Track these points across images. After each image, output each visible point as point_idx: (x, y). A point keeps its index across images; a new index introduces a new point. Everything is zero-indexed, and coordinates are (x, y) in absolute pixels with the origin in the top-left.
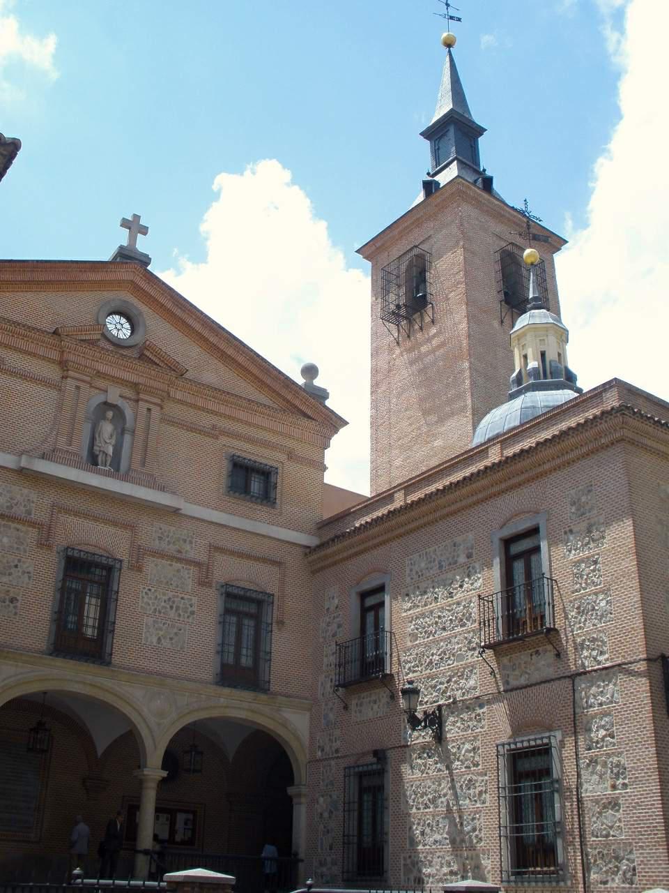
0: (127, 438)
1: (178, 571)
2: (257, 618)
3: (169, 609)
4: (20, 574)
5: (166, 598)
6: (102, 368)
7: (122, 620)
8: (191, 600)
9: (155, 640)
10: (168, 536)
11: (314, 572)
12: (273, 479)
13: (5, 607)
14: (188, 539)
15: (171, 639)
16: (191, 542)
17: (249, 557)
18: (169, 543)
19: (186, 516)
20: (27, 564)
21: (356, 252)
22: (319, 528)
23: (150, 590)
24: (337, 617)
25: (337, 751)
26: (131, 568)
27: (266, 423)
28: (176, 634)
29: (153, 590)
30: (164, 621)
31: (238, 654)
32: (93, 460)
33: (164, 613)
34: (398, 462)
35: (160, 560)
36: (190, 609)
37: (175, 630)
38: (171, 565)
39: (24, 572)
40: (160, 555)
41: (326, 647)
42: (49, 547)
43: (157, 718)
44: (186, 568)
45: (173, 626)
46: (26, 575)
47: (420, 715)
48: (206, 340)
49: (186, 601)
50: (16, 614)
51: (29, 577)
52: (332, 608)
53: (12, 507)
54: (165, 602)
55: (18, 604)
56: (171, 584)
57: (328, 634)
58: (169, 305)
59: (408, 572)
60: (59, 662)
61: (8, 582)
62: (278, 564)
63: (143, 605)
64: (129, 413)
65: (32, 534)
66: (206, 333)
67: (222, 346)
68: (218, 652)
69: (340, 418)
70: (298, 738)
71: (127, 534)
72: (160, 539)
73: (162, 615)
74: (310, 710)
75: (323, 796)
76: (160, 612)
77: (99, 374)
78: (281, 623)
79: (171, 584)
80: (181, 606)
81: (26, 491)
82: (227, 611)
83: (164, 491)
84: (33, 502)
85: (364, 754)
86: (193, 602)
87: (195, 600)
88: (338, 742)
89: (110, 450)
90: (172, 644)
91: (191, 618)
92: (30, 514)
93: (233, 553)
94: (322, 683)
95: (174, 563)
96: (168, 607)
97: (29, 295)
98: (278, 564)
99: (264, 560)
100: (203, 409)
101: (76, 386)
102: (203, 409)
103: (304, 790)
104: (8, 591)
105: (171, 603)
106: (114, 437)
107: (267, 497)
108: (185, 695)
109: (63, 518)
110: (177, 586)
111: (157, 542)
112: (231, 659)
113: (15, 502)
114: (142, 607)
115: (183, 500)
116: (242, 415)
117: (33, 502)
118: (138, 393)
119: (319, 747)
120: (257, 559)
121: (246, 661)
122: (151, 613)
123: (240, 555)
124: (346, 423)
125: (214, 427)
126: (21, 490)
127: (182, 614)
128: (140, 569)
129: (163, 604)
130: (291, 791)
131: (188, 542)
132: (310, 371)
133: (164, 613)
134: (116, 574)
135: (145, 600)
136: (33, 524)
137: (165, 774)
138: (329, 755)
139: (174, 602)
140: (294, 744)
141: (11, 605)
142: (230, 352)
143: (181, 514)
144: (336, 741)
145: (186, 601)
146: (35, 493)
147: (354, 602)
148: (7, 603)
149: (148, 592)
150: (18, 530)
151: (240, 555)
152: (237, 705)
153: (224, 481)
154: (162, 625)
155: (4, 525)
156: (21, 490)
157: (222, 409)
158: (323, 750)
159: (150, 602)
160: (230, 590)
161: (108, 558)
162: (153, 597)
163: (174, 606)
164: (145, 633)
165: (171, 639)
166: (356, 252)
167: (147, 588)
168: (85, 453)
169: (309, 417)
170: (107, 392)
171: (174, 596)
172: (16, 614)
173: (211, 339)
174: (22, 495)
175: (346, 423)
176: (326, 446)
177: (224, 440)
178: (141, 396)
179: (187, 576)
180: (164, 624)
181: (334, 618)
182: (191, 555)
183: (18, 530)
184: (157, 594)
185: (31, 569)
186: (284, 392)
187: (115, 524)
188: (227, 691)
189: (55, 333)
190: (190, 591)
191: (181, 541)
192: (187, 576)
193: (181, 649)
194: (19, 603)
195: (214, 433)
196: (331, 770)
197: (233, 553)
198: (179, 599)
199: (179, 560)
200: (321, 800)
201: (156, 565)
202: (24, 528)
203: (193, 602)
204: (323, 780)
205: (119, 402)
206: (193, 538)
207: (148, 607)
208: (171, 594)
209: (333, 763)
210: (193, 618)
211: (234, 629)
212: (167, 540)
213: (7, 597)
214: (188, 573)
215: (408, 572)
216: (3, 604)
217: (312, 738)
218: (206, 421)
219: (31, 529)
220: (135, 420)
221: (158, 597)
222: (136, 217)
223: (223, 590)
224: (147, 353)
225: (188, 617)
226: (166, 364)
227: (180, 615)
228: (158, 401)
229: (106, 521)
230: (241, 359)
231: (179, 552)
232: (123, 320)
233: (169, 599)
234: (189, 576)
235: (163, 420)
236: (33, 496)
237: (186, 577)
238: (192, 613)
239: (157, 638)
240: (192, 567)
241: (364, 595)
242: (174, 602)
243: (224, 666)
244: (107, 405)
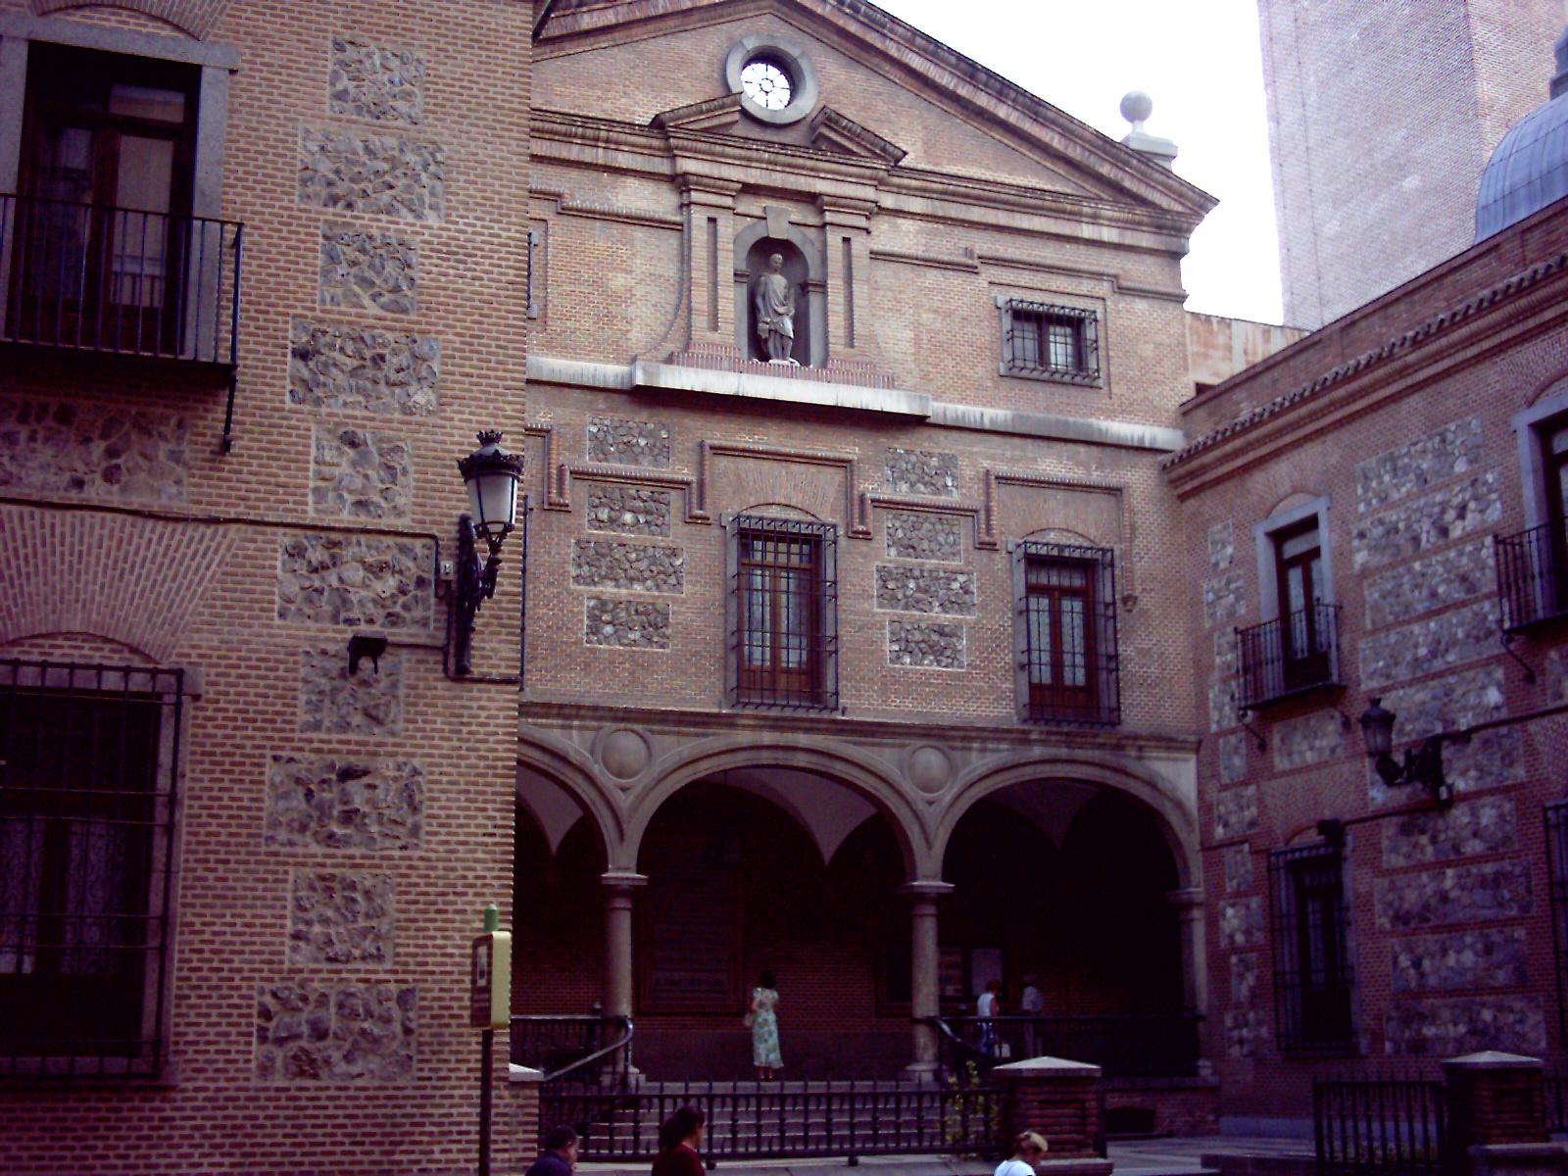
0: (814, 300)
2: (1087, 595)
11: (1183, 497)
22: (1185, 414)
26: (854, 535)
31: (1057, 665)
32: (759, 349)
34: (1331, 228)
43: (932, 795)
47: (1399, 758)
64: (810, 254)
69: (1204, 195)
70: (1179, 805)
82: (1032, 589)
85: (1300, 831)
107: (1082, 372)
108: (970, 749)
112: (1046, 676)
121: (1080, 678)
124: (1216, 202)
125: (968, 253)
132: (1134, 109)
134: (829, 552)
140: (1174, 818)
147: (1263, 554)
158: (1226, 825)
160: (1033, 550)
175: (1216, 202)
178: (829, 217)
205: (794, 236)
211: (1045, 619)
223: (1021, 552)
232: (773, 72)
241: (1279, 537)
243: (1035, 689)
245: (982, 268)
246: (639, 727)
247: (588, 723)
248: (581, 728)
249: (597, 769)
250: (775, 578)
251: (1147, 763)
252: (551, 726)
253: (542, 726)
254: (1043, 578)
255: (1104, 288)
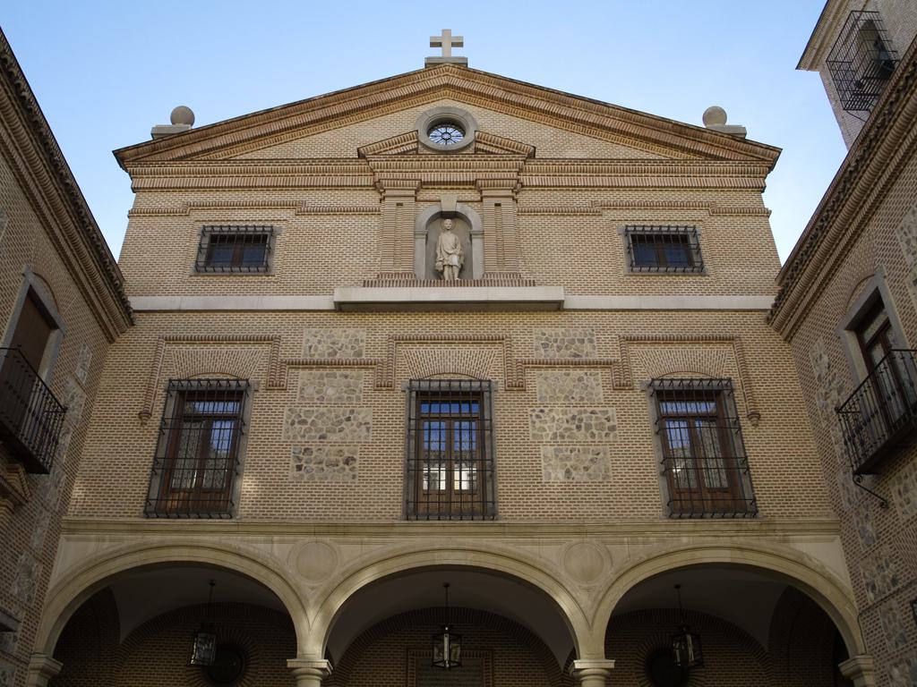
0: (477, 242)
1: (580, 379)
3: (575, 431)
4: (354, 427)
5: (570, 415)
6: (426, 177)
7: (505, 458)
8: (607, 412)
9: (561, 475)
10: (556, 341)
11: (788, 339)
12: (692, 241)
13: (338, 471)
14: (586, 339)
15: (586, 469)
16: (591, 341)
17: (681, 340)
18: (559, 348)
19: (576, 310)
20: (363, 415)
21: (797, 68)
23: (542, 411)
24: (833, 379)
25: (894, 581)
26: (510, 388)
27: (666, 181)
28: (592, 460)
29: (546, 410)
30: (570, 447)
32: (438, 276)
33: (569, 437)
35: (550, 371)
36: (608, 424)
37: (590, 456)
38: (568, 375)
39: (361, 424)
40: (552, 365)
41: (833, 430)
42: (389, 387)
44: (591, 374)
45: (586, 451)
46: (364, 427)
48: (559, 116)
49: (599, 415)
50: (354, 477)
51: (368, 429)
52: (825, 371)
53: (336, 353)
54: (567, 422)
55: (356, 465)
56: (573, 398)
57: (829, 410)
58: (500, 94)
59: (904, 247)
60: (419, 526)
61: (340, 441)
62: (730, 340)
63: (536, 432)
65: (363, 379)
66: (555, 109)
67: (580, 115)
68: (663, 474)
69: (768, 147)
70: (830, 580)
71: (497, 350)
72: (545, 346)
73: (566, 439)
74: (837, 531)
75: (896, 665)
76: (562, 437)
77: (424, 185)
78: (755, 416)
79: (573, 398)
80: (593, 422)
81: (351, 331)
82: (662, 419)
83: (534, 285)
84: (362, 341)
86: (610, 414)
87: (612, 411)
88: (891, 565)
89: (455, 260)
90: (589, 475)
91: (611, 436)
92: (361, 355)
93: (655, 341)
94: (843, 485)
95: (571, 371)
96: (574, 427)
97: (327, 135)
98: (730, 340)
99: (708, 340)
100: (574, 187)
101: (398, 204)
102: (574, 187)
103: (864, 662)
104: (341, 451)
105: (576, 422)
106: (459, 246)
109: (403, 349)
110: (582, 399)
111: (542, 351)
113: (340, 345)
114: (534, 435)
115: (562, 289)
116: (627, 181)
117: (362, 341)
118: (481, 191)
119: (867, 584)
120: (695, 340)
122: (549, 440)
123: (668, 341)
126: (345, 331)
127: (596, 432)
128: (521, 388)
129: (565, 425)
130: (845, 668)
131: (586, 342)
133: (569, 437)
135: (538, 425)
136: (365, 365)
137: (611, 664)
138: (884, 593)
139: (581, 420)
140: (826, 590)
141: (346, 467)
142: (592, 118)
143: (565, 310)
144: (888, 566)
145: (599, 415)
146: (364, 331)
148: (341, 465)
149: (541, 414)
150: (346, 377)
151: (668, 341)
152: (710, 543)
153: (622, 260)
154: (569, 452)
155: (327, 374)
156: (345, 331)
157: (599, 181)
159: (546, 426)
161: (471, 381)
162: (547, 419)
163: (583, 424)
164: (545, 469)
165: (586, 469)
166: (797, 68)
167: (537, 410)
168: (421, 272)
169: (722, 159)
170: (440, 201)
171: (580, 412)
172: (354, 477)
173: (563, 113)
174: (347, 337)
176: (762, 189)
177: (610, 215)
178: (484, 193)
179: (594, 383)
180: (571, 451)
181: (830, 383)
182: (596, 357)
183: (346, 377)
184: (553, 414)
185: (369, 419)
186: (677, 141)
187: (477, 341)
188: (687, 524)
189: (361, 156)
190: (602, 402)
191: (577, 343)
192: (594, 383)
193: (604, 479)
194: (358, 462)
195: (595, 211)
196: (894, 616)
197: (655, 341)
198: (588, 414)
199: (578, 365)
200: (896, 672)
201: (546, 379)
202: (355, 373)
203: (610, 414)
204: (889, 637)
205: (459, 208)
206: (593, 335)
207: (544, 433)
208: (574, 411)
209: (894, 603)
210: (615, 436)
212: (555, 345)
213: (340, 458)
214: (595, 380)
215: (904, 247)
216: (335, 468)
217: (854, 576)
218: (582, 200)
219: (363, 371)
220: (483, 221)
221: (557, 418)
222: (446, 32)
224: (481, 146)
225: (607, 435)
226: (507, 150)
227: (593, 435)
228: (509, 193)
229: (464, 340)
230: (609, 123)
231: (576, 355)
233: (574, 418)
234: (598, 382)
235: (521, 213)
236: (362, 335)
237: (594, 385)
238: (613, 428)
239: (564, 471)
240: (599, 371)
241: (858, 326)
242: (581, 420)
244: (443, 215)
245: (605, 213)
246: (327, 539)
247: (286, 538)
248: (281, 542)
249: (290, 571)
250: (450, 429)
251: (792, 545)
252: (256, 542)
253: (252, 541)
254: (670, 408)
255: (702, 214)
